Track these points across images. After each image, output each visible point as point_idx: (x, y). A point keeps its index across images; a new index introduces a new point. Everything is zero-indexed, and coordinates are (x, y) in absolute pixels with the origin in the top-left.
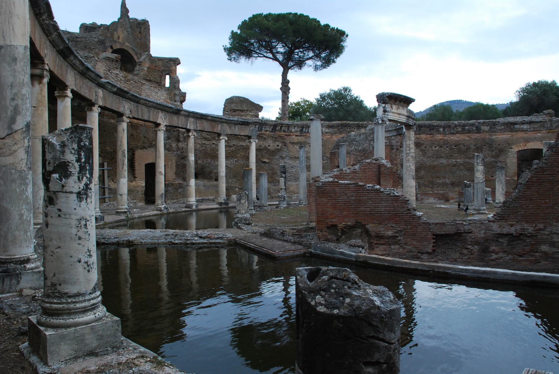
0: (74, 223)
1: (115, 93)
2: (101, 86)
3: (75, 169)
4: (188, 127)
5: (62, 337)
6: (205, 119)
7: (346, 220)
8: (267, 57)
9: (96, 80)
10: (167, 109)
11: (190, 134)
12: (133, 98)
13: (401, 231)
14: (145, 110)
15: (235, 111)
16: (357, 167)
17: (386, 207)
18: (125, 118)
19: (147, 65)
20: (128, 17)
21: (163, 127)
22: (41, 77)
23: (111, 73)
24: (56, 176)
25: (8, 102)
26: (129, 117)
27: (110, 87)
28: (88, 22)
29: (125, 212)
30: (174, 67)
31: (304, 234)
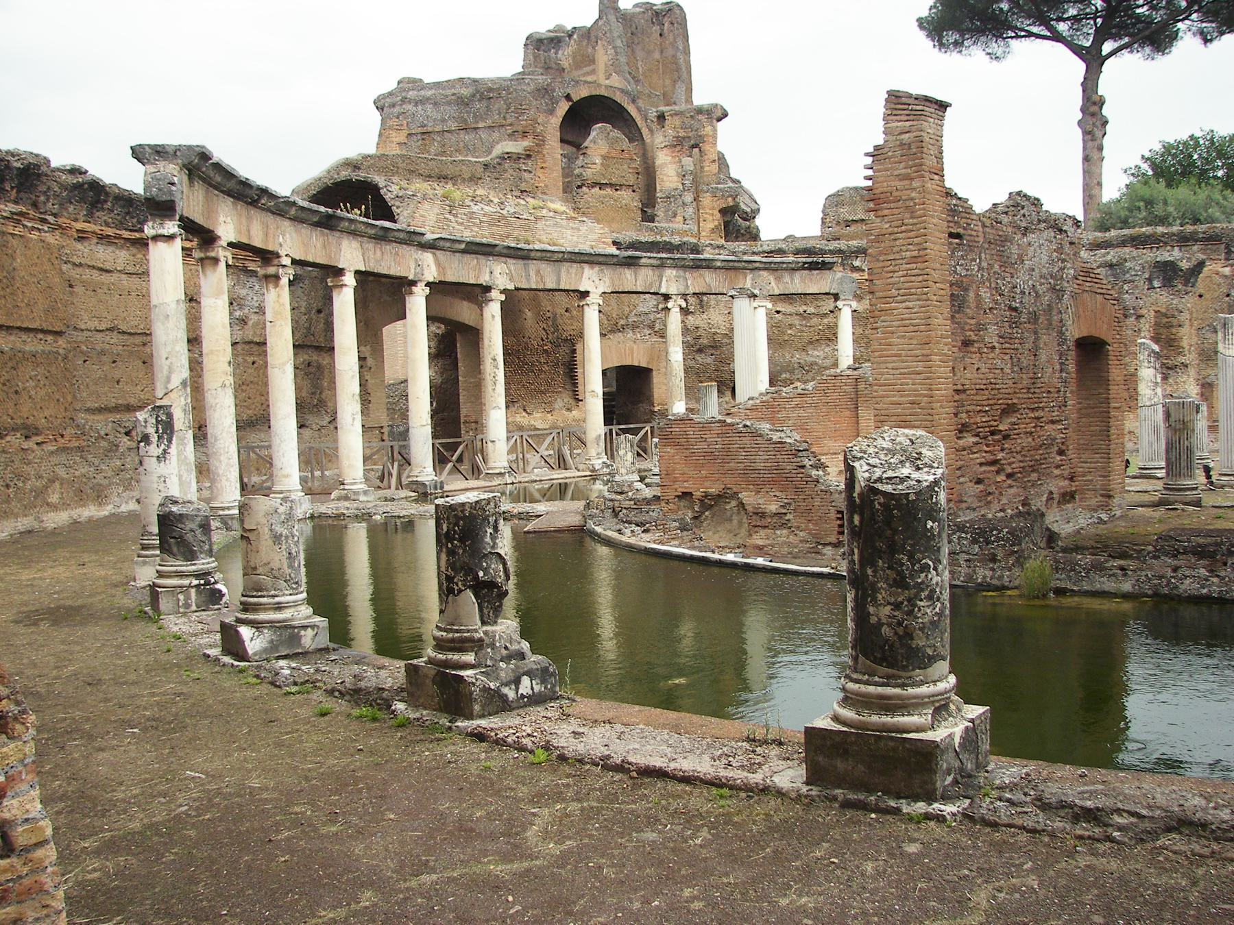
0: (156, 479)
1: (463, 252)
2: (431, 246)
3: (154, 438)
4: (663, 291)
5: (145, 563)
6: (708, 267)
7: (707, 484)
8: (1038, 36)
9: (413, 239)
10: (601, 259)
11: (670, 305)
12: (512, 251)
13: (790, 504)
14: (546, 268)
15: (848, 223)
16: (810, 386)
17: (766, 461)
18: (494, 294)
19: (603, 152)
20: (617, 9)
21: (595, 298)
22: (277, 278)
23: (455, 216)
24: (142, 444)
25: (163, 359)
26: (503, 292)
27: (448, 244)
28: (543, 27)
29: (500, 474)
30: (708, 129)
31: (645, 508)
